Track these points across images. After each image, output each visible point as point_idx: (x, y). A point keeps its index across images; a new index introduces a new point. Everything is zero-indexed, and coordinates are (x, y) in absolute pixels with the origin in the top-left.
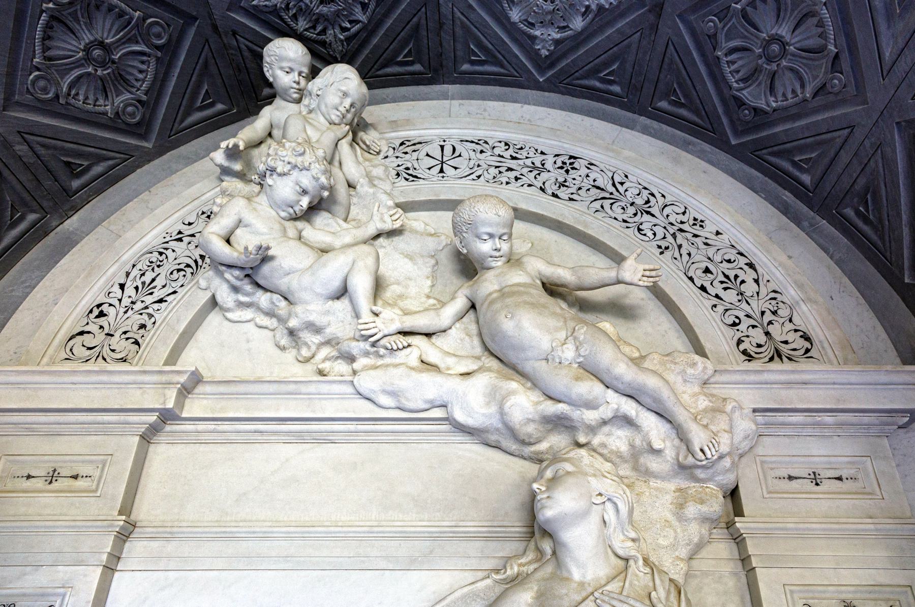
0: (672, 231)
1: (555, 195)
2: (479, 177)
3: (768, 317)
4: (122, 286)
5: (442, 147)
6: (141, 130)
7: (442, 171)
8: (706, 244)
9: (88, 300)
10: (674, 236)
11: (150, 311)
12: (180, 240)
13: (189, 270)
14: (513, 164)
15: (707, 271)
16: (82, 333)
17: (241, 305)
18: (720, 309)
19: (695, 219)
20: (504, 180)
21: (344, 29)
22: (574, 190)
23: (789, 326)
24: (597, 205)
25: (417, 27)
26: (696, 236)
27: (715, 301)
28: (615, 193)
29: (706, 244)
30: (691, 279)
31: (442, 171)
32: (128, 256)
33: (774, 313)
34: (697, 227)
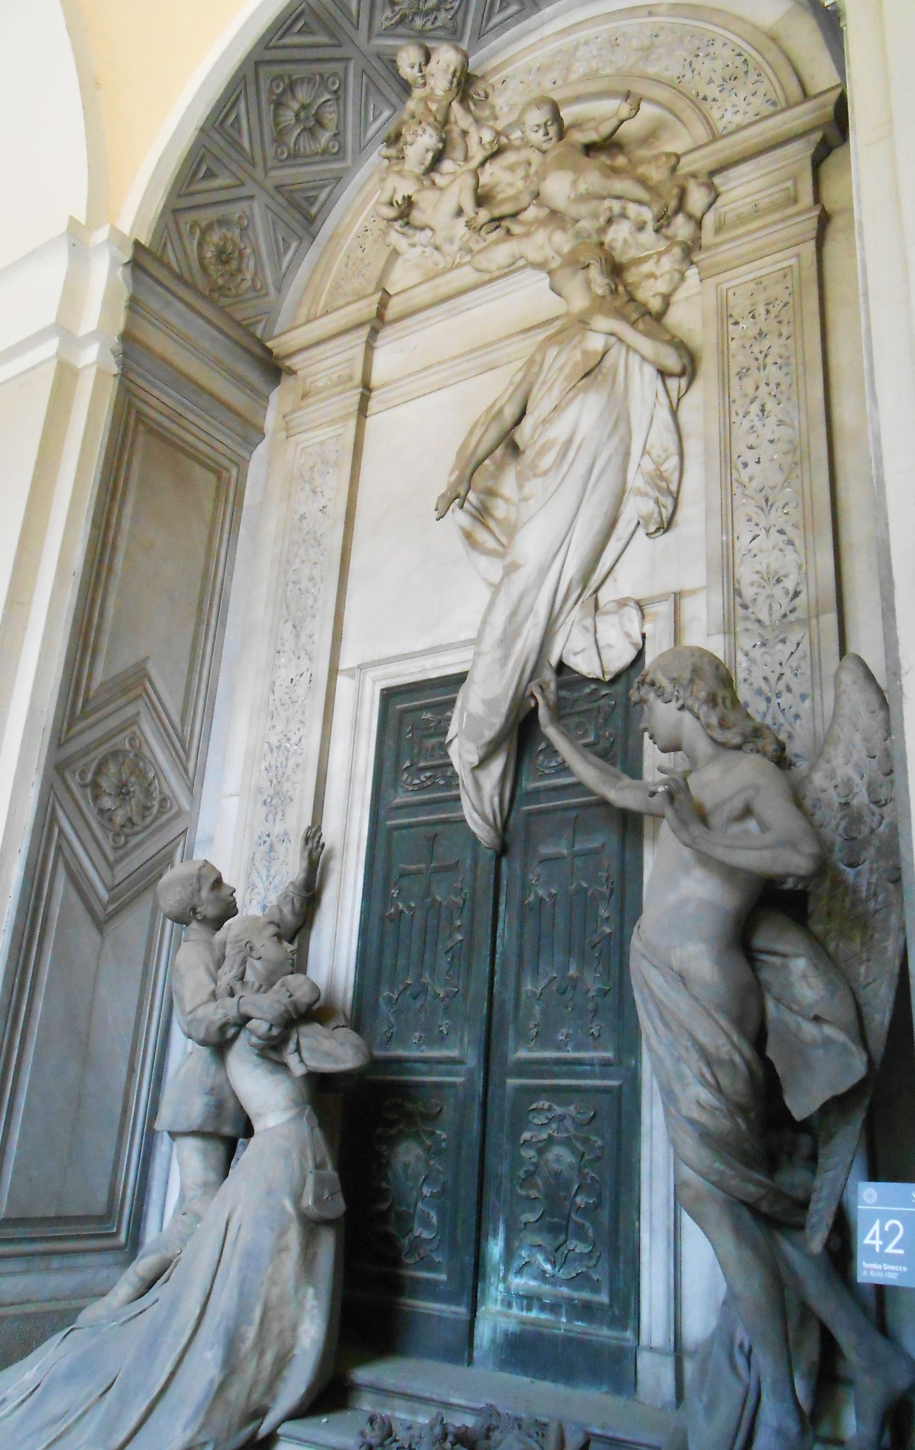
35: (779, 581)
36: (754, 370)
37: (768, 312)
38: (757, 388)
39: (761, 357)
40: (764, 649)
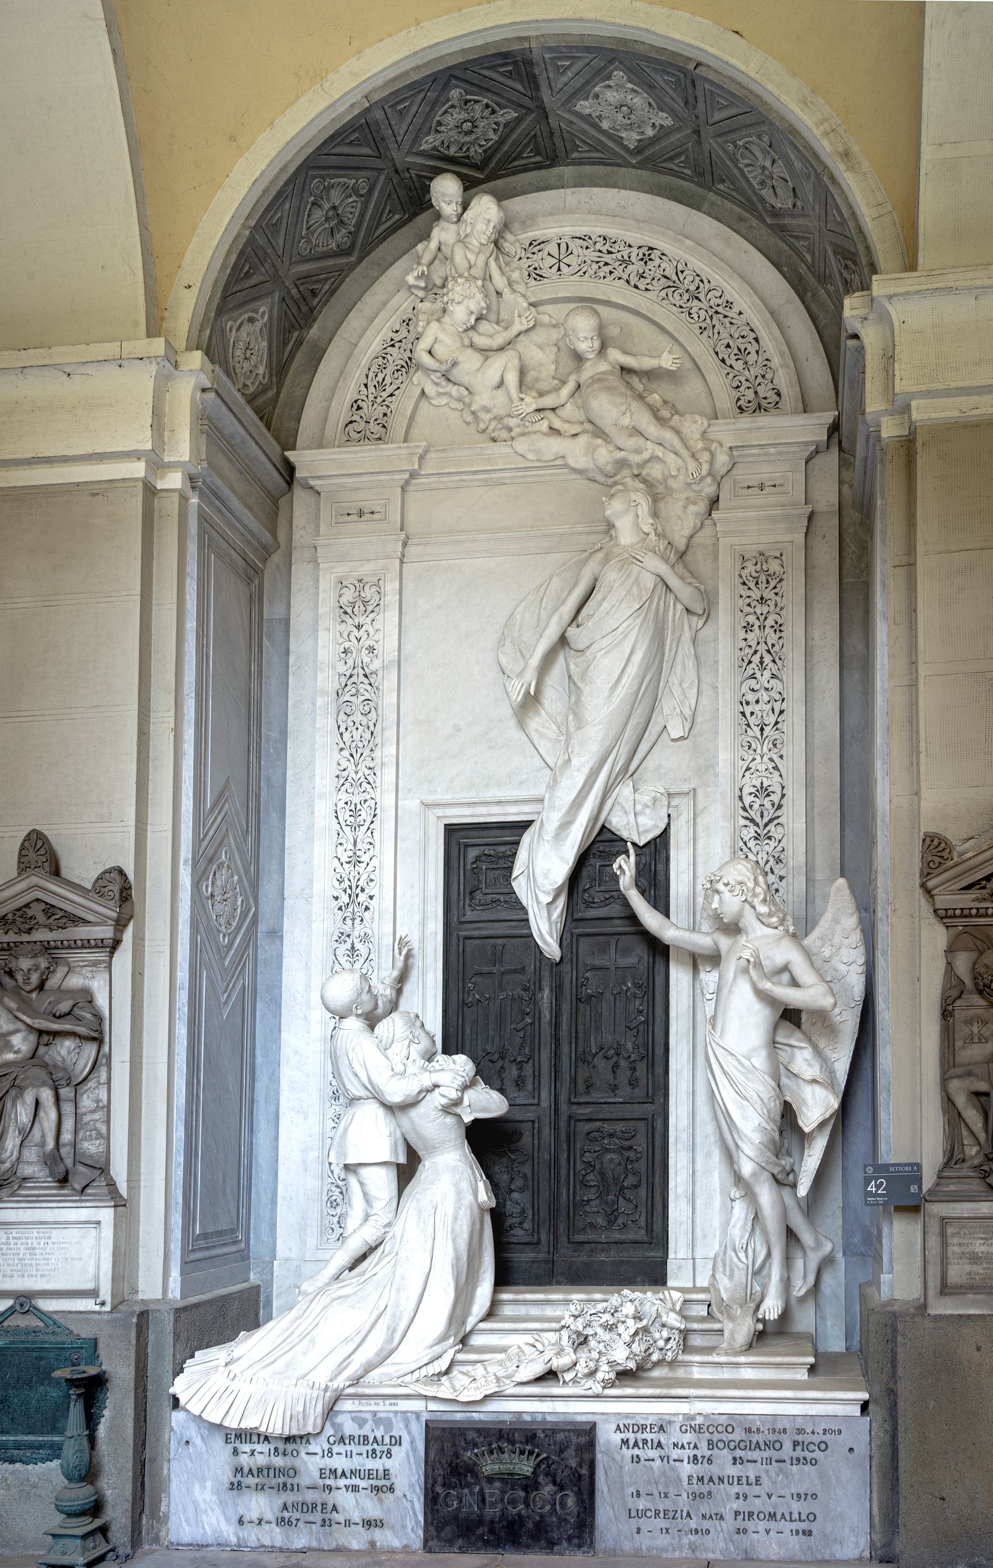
0: (710, 314)
1: (636, 287)
2: (585, 273)
3: (759, 379)
4: (366, 385)
5: (559, 245)
6: (347, 252)
7: (559, 270)
8: (731, 323)
9: (349, 399)
10: (711, 317)
11: (386, 403)
12: (393, 346)
13: (403, 370)
14: (608, 258)
15: (728, 346)
16: (351, 422)
17: (439, 394)
18: (731, 376)
19: (727, 302)
20: (602, 274)
21: (481, 146)
22: (648, 281)
23: (770, 386)
24: (663, 293)
25: (535, 135)
26: (725, 317)
27: (729, 370)
28: (678, 282)
29: (731, 323)
30: (717, 353)
31: (559, 270)
32: (365, 361)
33: (763, 376)
34: (727, 309)
35: (768, 795)
36: (756, 627)
37: (768, 582)
38: (758, 643)
39: (762, 618)
40: (757, 842)
